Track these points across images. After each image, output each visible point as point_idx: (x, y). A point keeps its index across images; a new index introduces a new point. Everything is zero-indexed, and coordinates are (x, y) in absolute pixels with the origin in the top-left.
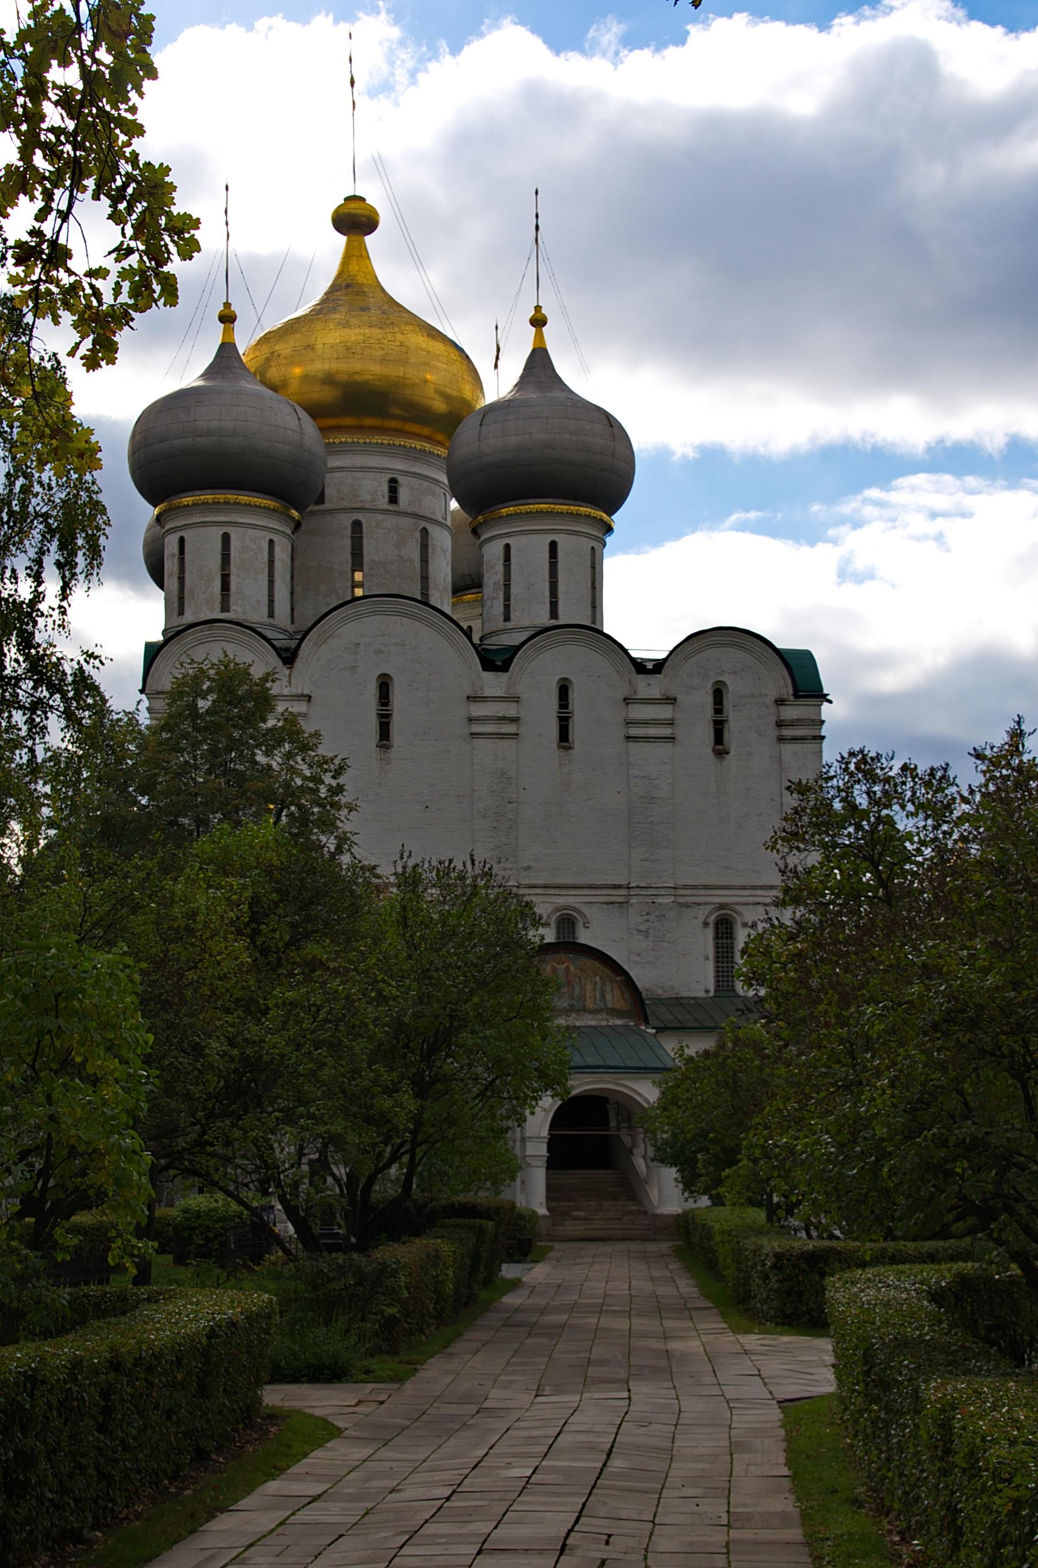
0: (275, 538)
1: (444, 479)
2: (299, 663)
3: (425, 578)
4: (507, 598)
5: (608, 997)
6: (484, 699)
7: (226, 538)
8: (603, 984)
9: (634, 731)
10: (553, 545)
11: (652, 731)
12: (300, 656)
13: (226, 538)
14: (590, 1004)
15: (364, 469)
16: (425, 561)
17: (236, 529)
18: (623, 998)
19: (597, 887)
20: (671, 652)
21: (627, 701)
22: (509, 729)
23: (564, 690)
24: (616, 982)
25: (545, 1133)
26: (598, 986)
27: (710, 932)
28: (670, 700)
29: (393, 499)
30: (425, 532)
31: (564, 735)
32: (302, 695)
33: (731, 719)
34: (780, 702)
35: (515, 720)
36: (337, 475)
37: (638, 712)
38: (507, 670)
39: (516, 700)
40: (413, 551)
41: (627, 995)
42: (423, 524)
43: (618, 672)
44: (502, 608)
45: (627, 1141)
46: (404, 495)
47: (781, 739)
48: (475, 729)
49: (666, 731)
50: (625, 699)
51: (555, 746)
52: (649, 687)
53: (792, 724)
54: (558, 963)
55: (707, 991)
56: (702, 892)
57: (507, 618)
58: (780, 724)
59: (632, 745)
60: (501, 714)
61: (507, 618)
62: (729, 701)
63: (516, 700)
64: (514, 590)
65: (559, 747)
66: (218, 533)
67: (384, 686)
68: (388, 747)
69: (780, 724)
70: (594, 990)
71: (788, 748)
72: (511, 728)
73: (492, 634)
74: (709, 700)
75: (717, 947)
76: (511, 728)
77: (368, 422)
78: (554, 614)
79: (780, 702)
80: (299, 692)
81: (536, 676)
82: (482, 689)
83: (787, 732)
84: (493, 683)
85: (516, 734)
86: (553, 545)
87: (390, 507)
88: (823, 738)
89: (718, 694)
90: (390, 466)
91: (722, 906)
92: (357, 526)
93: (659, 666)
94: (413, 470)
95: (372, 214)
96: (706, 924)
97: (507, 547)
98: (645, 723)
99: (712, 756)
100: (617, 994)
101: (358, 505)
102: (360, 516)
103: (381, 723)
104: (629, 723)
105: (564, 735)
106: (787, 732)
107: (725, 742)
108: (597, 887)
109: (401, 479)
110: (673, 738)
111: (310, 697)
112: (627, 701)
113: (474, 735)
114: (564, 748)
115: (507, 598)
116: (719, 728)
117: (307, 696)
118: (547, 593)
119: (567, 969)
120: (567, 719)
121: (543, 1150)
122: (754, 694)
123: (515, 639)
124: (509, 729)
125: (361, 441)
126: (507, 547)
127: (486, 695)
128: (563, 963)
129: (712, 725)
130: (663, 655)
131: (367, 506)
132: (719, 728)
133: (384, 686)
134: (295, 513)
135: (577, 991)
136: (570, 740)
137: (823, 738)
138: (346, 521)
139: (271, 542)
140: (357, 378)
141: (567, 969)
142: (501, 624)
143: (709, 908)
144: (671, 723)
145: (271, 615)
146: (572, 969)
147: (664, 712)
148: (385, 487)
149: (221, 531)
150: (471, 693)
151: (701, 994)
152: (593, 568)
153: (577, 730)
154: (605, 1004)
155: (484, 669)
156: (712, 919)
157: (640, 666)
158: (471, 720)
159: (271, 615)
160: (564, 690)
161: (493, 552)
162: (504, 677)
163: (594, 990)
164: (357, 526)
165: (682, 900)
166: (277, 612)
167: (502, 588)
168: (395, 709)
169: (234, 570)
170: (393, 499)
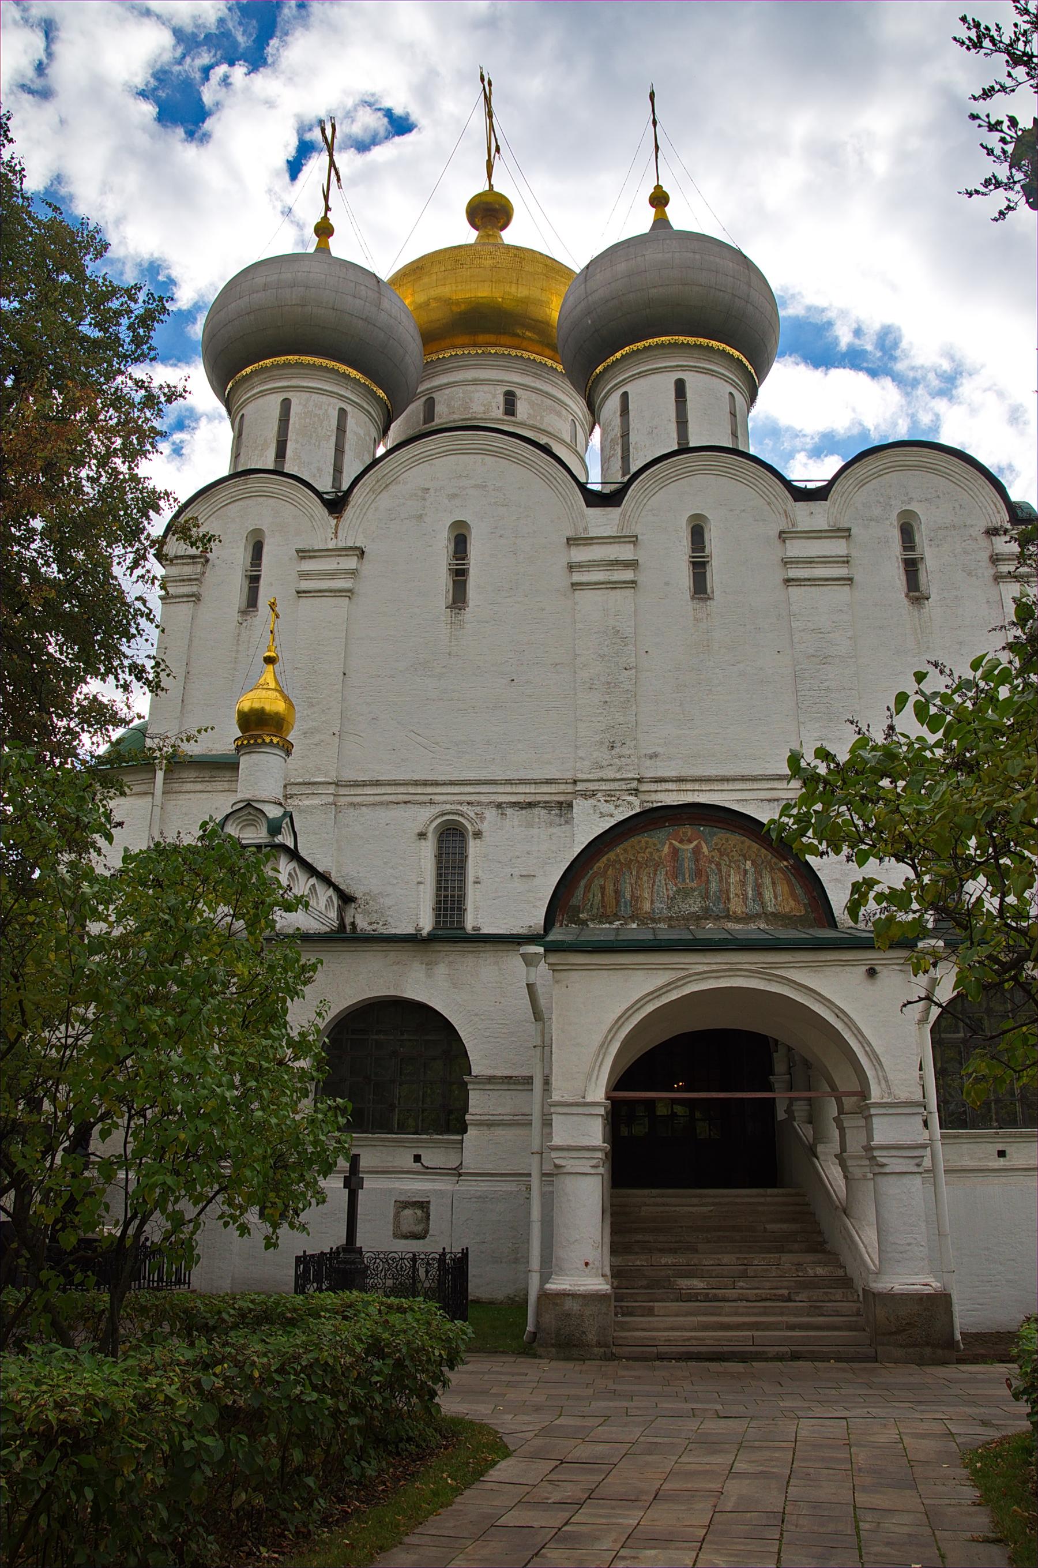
0: (349, 408)
2: (349, 512)
5: (768, 895)
6: (590, 541)
7: (286, 404)
8: (758, 873)
10: (680, 387)
12: (352, 503)
13: (286, 404)
14: (736, 906)
15: (476, 382)
17: (298, 394)
18: (793, 894)
19: (754, 779)
21: (783, 536)
22: (625, 576)
23: (698, 533)
24: (780, 869)
25: (598, 1093)
26: (751, 878)
28: (844, 533)
31: (700, 588)
32: (351, 548)
33: (927, 555)
35: (632, 565)
36: (447, 391)
37: (796, 549)
38: (618, 504)
39: (634, 540)
41: (799, 891)
43: (769, 504)
44: (620, 463)
45: (806, 1132)
46: (522, 409)
48: (577, 577)
50: (781, 532)
51: (688, 596)
52: (811, 516)
54: (681, 842)
59: (794, 591)
60: (612, 558)
62: (922, 538)
63: (634, 540)
64: (633, 438)
65: (693, 598)
66: (277, 399)
70: (743, 884)
72: (628, 575)
74: (896, 534)
76: (628, 575)
80: (350, 544)
81: (658, 516)
82: (586, 529)
84: (602, 521)
85: (633, 582)
86: (680, 387)
87: (505, 417)
89: (907, 533)
90: (506, 379)
94: (533, 384)
95: (503, 202)
97: (625, 395)
98: (810, 562)
99: (906, 602)
100: (782, 888)
101: (469, 416)
104: (786, 563)
105: (700, 588)
107: (923, 588)
108: (754, 779)
109: (519, 392)
110: (851, 579)
111: (363, 552)
112: (783, 536)
116: (912, 567)
117: (357, 548)
118: (675, 435)
119: (697, 851)
120: (703, 564)
121: (594, 1133)
124: (625, 576)
125: (473, 352)
127: (591, 535)
128: (690, 841)
129: (901, 565)
131: (479, 416)
132: (912, 567)
134: (381, 393)
135: (714, 886)
136: (709, 591)
139: (342, 413)
141: (697, 851)
144: (846, 561)
146: (705, 850)
147: (837, 547)
148: (501, 399)
149: (279, 398)
150: (570, 533)
153: (715, 576)
154: (763, 905)
157: (802, 495)
158: (571, 567)
160: (698, 533)
162: (614, 513)
163: (743, 884)
167: (620, 441)
168: (472, 562)
169: (291, 436)
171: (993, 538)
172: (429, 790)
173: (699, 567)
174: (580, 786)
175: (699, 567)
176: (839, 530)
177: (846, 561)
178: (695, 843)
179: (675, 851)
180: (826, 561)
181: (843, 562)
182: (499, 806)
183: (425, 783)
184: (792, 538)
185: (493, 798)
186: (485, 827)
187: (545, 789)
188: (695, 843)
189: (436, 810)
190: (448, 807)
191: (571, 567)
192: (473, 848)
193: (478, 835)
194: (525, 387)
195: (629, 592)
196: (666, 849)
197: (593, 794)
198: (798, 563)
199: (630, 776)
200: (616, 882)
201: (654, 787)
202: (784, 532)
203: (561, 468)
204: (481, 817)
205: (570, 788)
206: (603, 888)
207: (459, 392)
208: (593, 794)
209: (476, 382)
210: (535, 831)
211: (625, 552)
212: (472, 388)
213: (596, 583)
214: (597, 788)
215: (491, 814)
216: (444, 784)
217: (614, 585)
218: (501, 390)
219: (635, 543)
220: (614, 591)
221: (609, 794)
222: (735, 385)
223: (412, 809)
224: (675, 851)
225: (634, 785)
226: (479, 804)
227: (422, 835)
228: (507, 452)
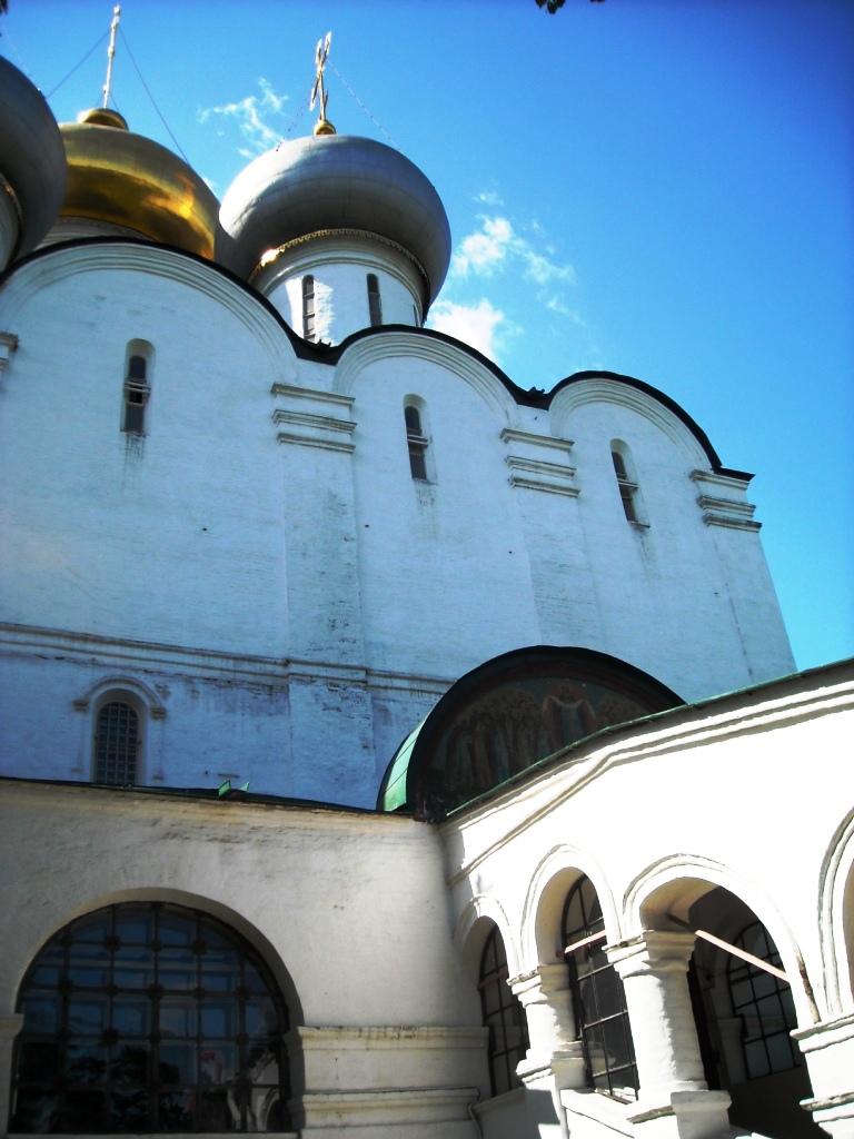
11: (546, 478)
22: (339, 435)
28: (565, 444)
31: (418, 470)
35: (349, 427)
39: (349, 402)
48: (284, 428)
54: (562, 698)
63: (349, 402)
72: (344, 438)
76: (344, 438)
88: (759, 525)
124: (339, 435)
128: (573, 700)
133: (138, 367)
147: (558, 457)
171: (700, 483)
172: (90, 647)
173: (417, 451)
174: (294, 668)
175: (417, 451)
176: (561, 441)
178: (579, 702)
179: (557, 711)
180: (552, 467)
181: (568, 474)
182: (189, 680)
183: (85, 638)
184: (515, 439)
185: (180, 669)
186: (168, 705)
187: (246, 666)
188: (579, 702)
189: (100, 674)
190: (118, 672)
191: (279, 416)
192: (152, 731)
193: (160, 714)
195: (346, 457)
196: (545, 706)
197: (312, 679)
198: (524, 464)
199: (355, 663)
200: (489, 743)
201: (383, 682)
202: (508, 431)
203: (268, 314)
204: (165, 693)
205: (279, 670)
206: (471, 749)
208: (312, 679)
210: (238, 718)
211: (342, 414)
213: (308, 439)
214: (316, 673)
215: (177, 690)
216: (113, 642)
217: (331, 446)
219: (350, 406)
220: (329, 453)
221: (332, 684)
223: (65, 670)
224: (557, 711)
225: (362, 675)
226: (160, 673)
227: (80, 705)
228: (204, 283)
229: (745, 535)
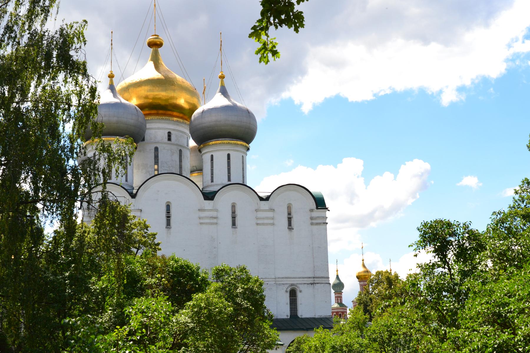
1: (188, 132)
3: (181, 167)
4: (212, 174)
9: (260, 222)
10: (229, 156)
11: (266, 221)
15: (159, 129)
16: (181, 161)
20: (272, 193)
27: (288, 294)
28: (272, 210)
29: (169, 139)
30: (180, 151)
31: (234, 224)
34: (312, 210)
37: (260, 214)
39: (217, 210)
40: (176, 157)
42: (180, 148)
46: (173, 137)
47: (312, 224)
48: (202, 221)
49: (271, 221)
53: (316, 218)
55: (287, 316)
56: (285, 280)
57: (212, 181)
58: (312, 218)
59: (259, 227)
61: (212, 181)
63: (217, 210)
65: (232, 227)
67: (168, 207)
68: (170, 228)
69: (312, 218)
71: (315, 227)
72: (215, 221)
73: (208, 186)
75: (290, 300)
77: (161, 112)
78: (229, 180)
79: (312, 210)
83: (314, 221)
86: (229, 156)
88: (327, 223)
91: (292, 285)
92: (156, 149)
93: (268, 198)
96: (286, 291)
97: (212, 156)
98: (263, 218)
99: (287, 230)
102: (157, 145)
103: (167, 220)
105: (234, 224)
106: (314, 221)
109: (172, 132)
113: (201, 223)
114: (234, 228)
115: (212, 174)
116: (290, 219)
120: (235, 217)
122: (303, 208)
123: (215, 189)
126: (212, 156)
129: (287, 219)
130: (269, 194)
132: (290, 219)
133: (168, 207)
137: (327, 223)
138: (153, 147)
140: (157, 96)
142: (210, 183)
143: (288, 285)
144: (273, 218)
145: (126, 181)
147: (270, 214)
148: (167, 135)
151: (285, 317)
152: (243, 163)
155: (205, 199)
156: (289, 290)
157: (261, 199)
159: (126, 181)
161: (207, 158)
164: (156, 149)
165: (278, 283)
166: (128, 180)
170: (169, 139)
177: (273, 218)
180: (267, 218)
194: (174, 130)
207: (153, 131)
209: (159, 129)
211: (214, 214)
212: (157, 129)
217: (212, 224)
218: (167, 131)
222: (244, 153)
229: (322, 227)
